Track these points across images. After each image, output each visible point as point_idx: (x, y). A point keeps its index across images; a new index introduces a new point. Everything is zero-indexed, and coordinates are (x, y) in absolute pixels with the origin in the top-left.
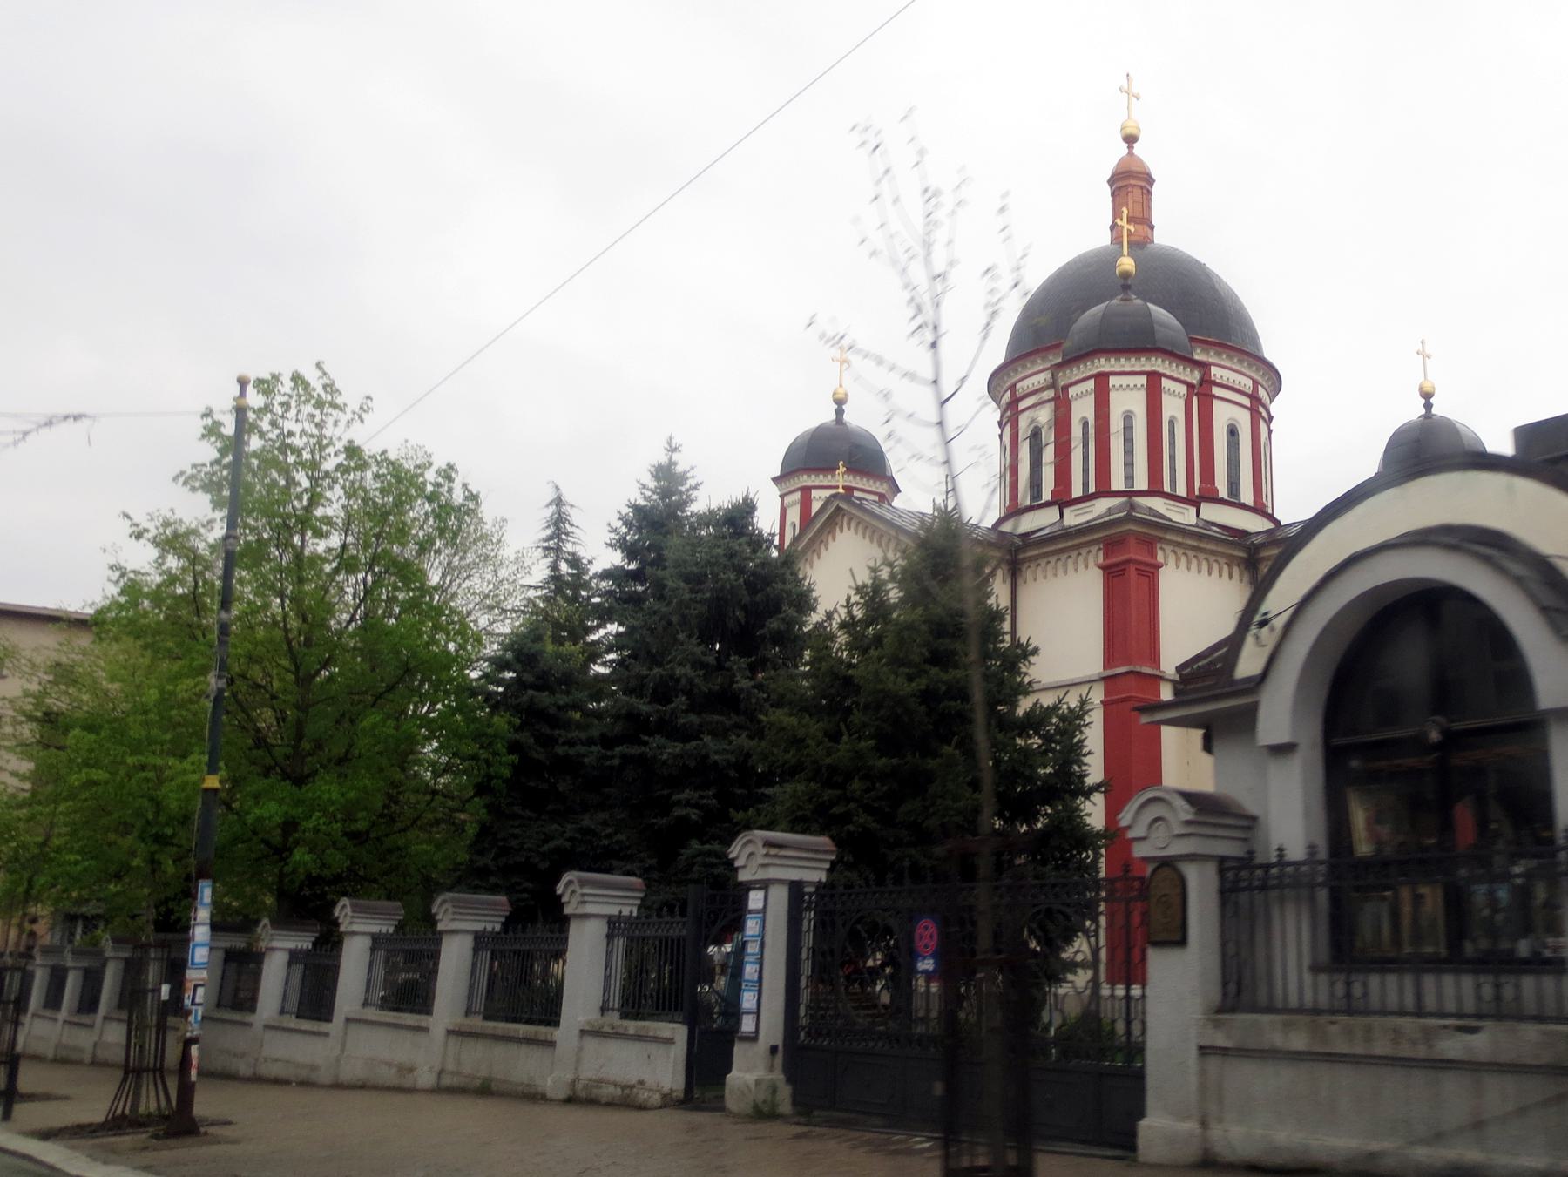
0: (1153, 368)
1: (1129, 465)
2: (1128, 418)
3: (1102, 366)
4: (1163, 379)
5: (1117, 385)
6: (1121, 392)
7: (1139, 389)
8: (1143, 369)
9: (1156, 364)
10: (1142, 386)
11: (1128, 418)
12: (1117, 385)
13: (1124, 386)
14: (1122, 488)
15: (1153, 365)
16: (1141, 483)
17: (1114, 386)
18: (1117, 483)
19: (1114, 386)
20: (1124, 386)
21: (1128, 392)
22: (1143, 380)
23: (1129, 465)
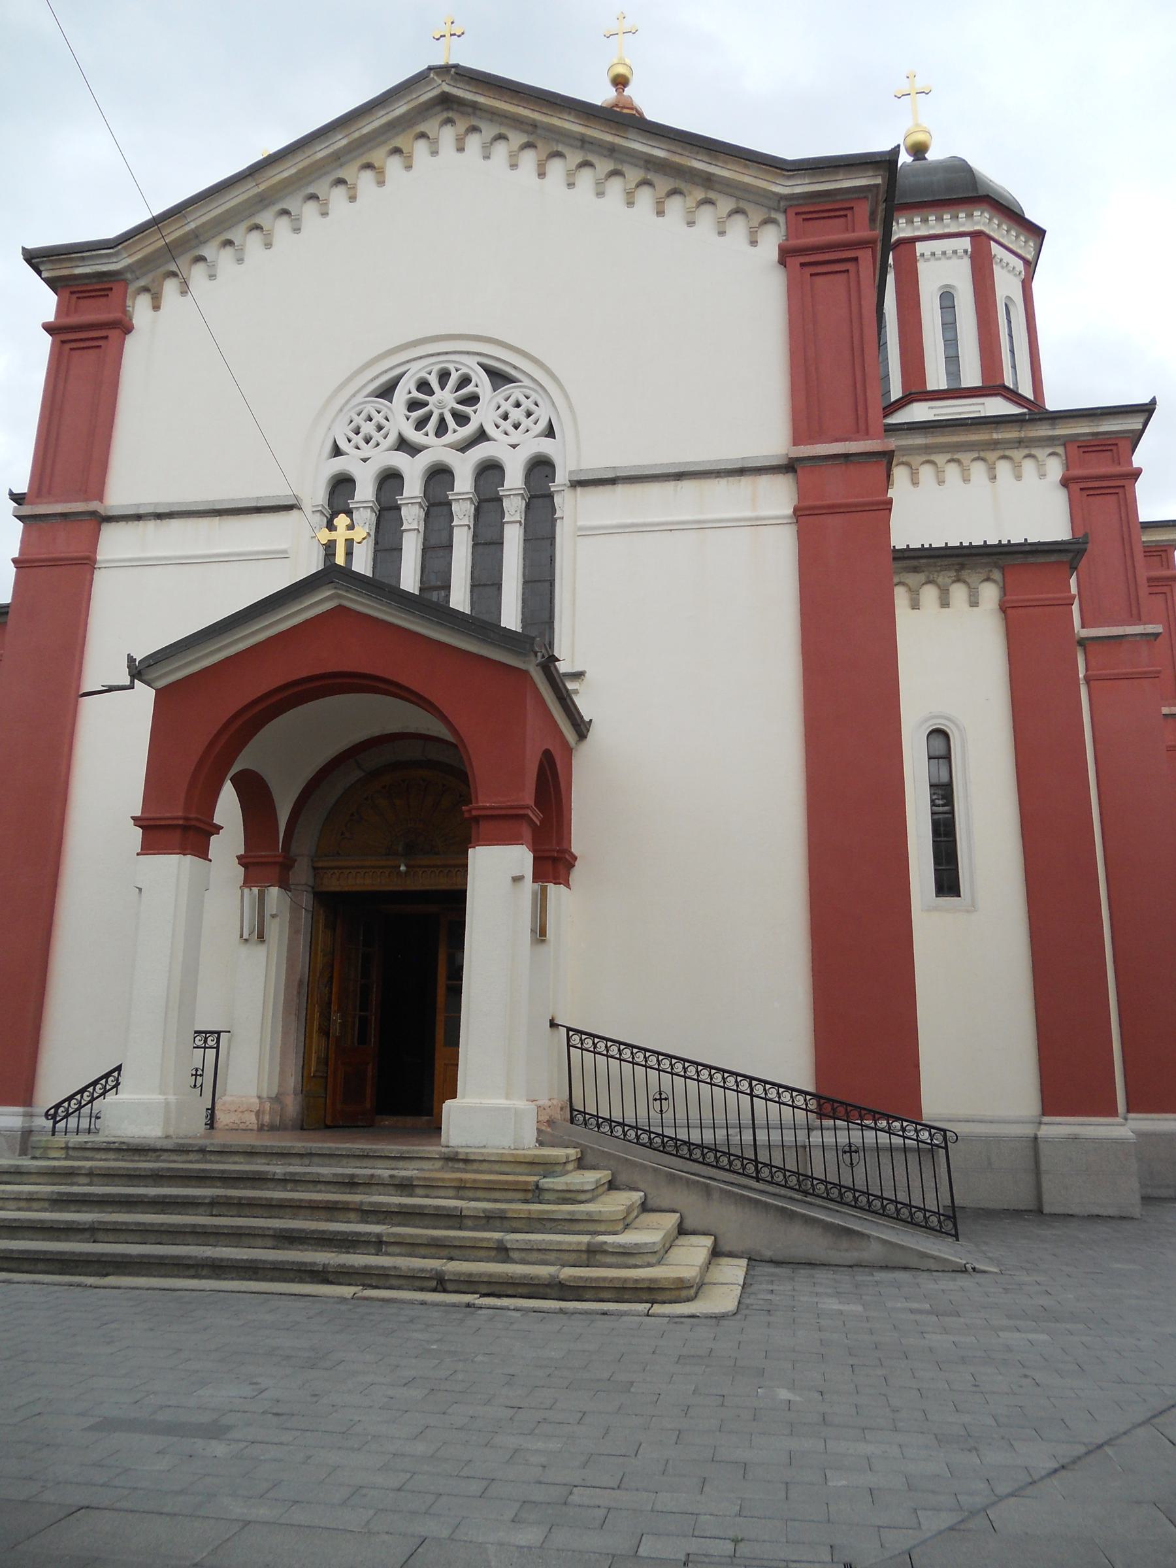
0: (977, 228)
1: (952, 360)
2: (947, 299)
3: (903, 230)
4: (992, 242)
5: (927, 254)
6: (933, 263)
7: (961, 258)
8: (962, 229)
9: (981, 220)
10: (966, 251)
11: (947, 299)
12: (927, 254)
13: (938, 253)
14: (943, 386)
15: (978, 223)
16: (971, 377)
17: (922, 255)
18: (936, 379)
19: (922, 255)
20: (938, 253)
21: (944, 262)
22: (966, 243)
23: (952, 360)
